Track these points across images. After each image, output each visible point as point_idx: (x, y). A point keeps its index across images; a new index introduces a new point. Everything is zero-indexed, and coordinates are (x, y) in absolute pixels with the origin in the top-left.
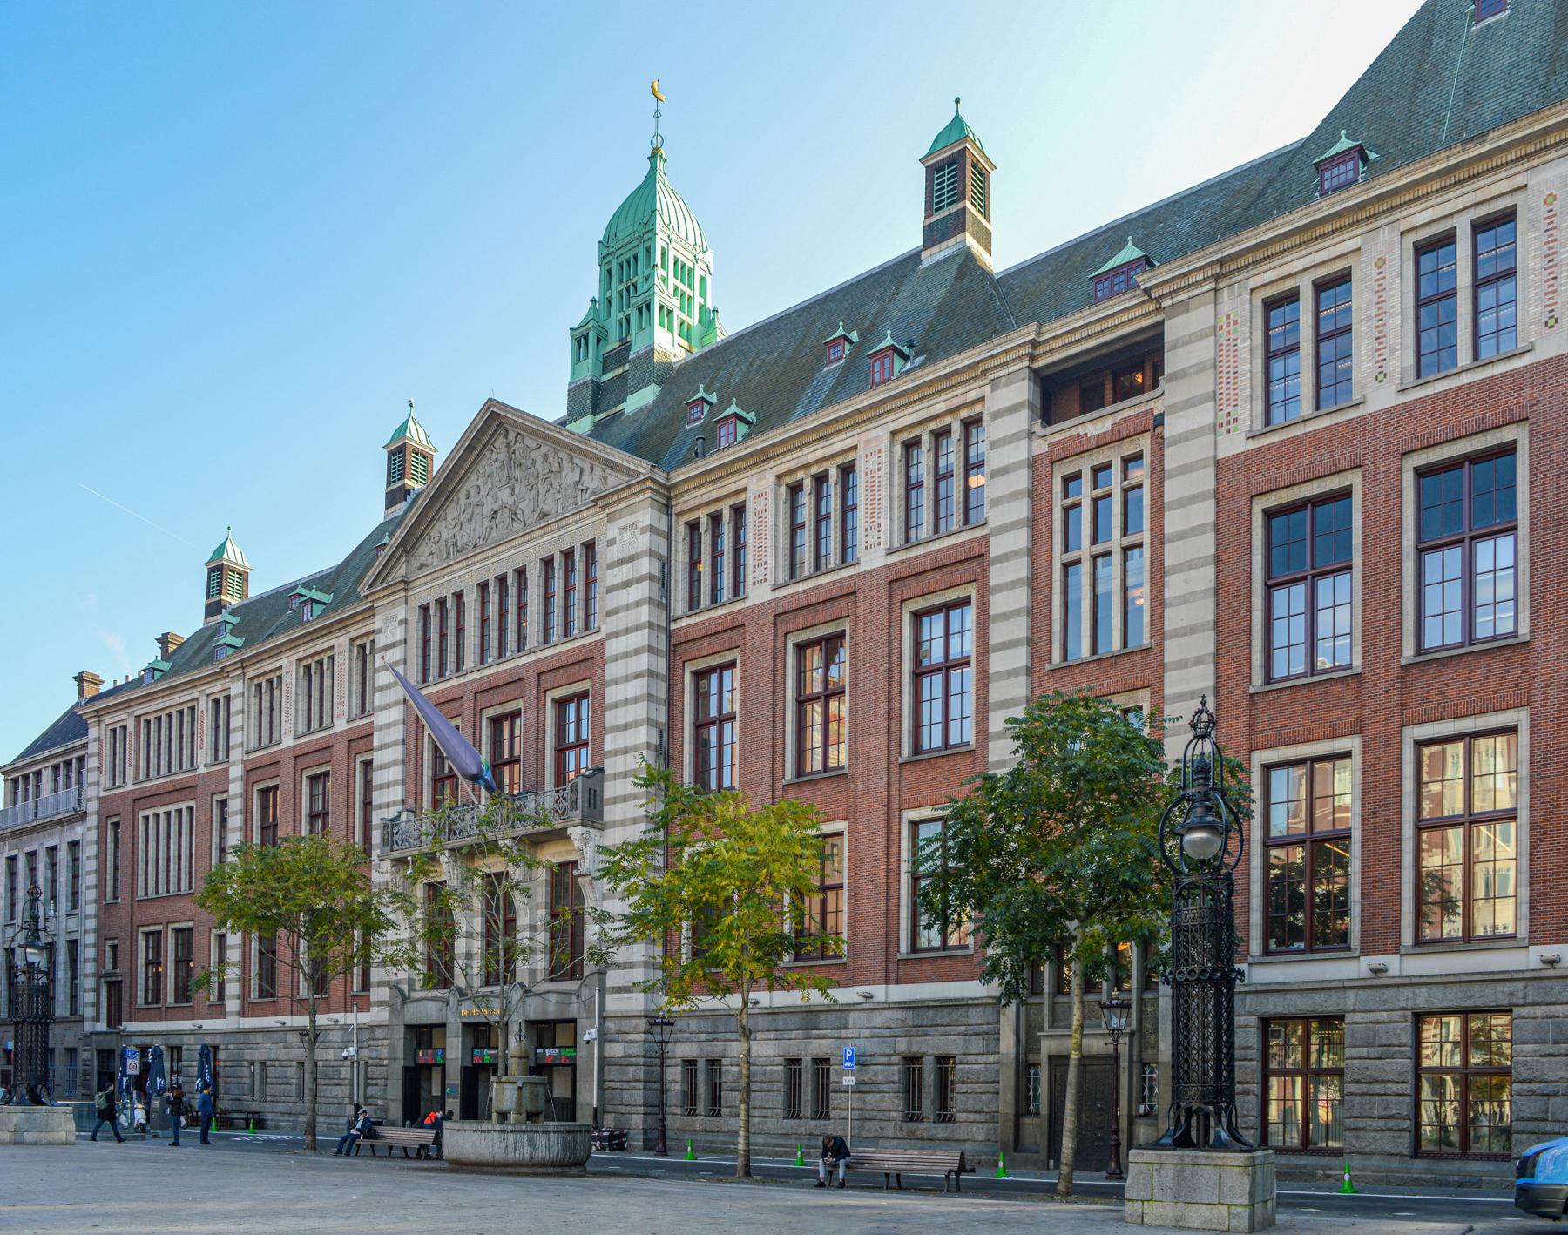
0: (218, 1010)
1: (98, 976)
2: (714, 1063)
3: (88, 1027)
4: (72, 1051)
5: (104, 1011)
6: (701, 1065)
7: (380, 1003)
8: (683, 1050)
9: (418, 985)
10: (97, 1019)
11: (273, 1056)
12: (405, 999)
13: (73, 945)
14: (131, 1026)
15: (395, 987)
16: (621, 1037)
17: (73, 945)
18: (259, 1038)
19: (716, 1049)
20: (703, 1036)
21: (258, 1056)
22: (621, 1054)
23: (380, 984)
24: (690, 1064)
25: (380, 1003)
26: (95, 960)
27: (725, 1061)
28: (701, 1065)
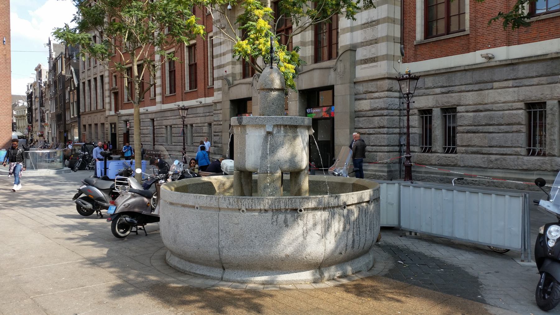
0: (153, 102)
1: (110, 90)
2: (449, 112)
3: (107, 113)
4: (103, 124)
5: (113, 106)
6: (437, 114)
7: (219, 89)
8: (421, 102)
9: (238, 77)
10: (110, 110)
11: (175, 123)
12: (231, 86)
13: (102, 77)
14: (122, 112)
15: (224, 78)
16: (368, 96)
17: (102, 77)
18: (169, 114)
19: (450, 100)
20: (438, 90)
21: (168, 122)
22: (368, 108)
23: (218, 79)
24: (426, 114)
25: (219, 89)
26: (109, 83)
27: (459, 109)
28: (437, 114)
